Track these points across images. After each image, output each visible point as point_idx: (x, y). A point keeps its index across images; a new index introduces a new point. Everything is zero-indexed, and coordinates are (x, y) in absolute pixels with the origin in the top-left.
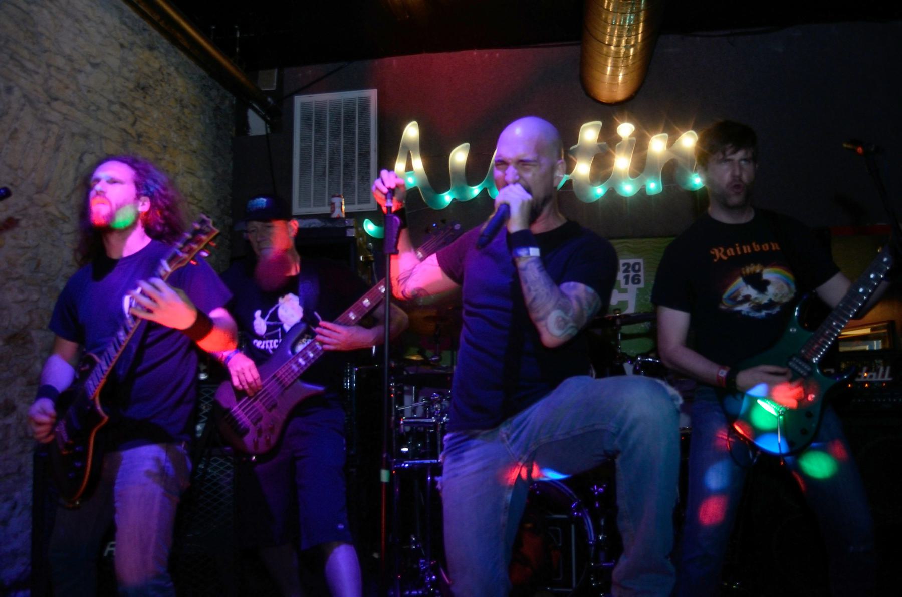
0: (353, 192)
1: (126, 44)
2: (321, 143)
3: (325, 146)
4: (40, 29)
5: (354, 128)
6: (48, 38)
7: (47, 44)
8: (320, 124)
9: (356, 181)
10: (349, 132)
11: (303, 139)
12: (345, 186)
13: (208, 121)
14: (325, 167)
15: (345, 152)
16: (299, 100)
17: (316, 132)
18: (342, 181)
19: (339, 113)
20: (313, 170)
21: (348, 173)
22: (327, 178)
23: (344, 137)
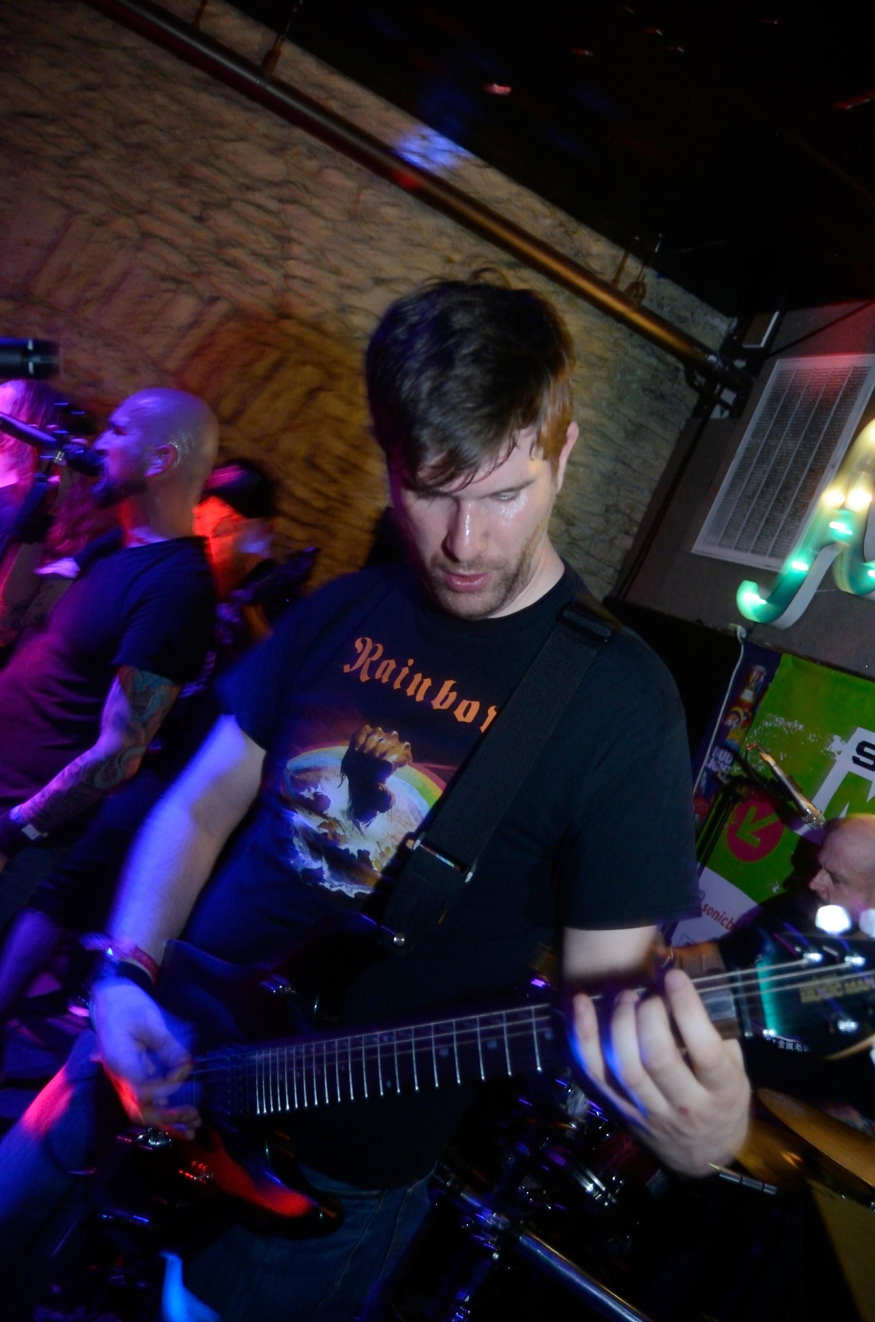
0: (773, 536)
1: (457, 257)
2: (773, 443)
3: (776, 446)
4: (293, 234)
5: (824, 423)
6: (300, 243)
7: (297, 250)
8: (786, 410)
9: (785, 516)
10: (815, 428)
11: (755, 435)
12: (767, 521)
13: (634, 386)
14: (759, 485)
15: (795, 461)
16: (781, 365)
17: (775, 424)
18: (767, 515)
19: (817, 393)
20: (744, 485)
21: (781, 501)
22: (753, 503)
23: (804, 437)
